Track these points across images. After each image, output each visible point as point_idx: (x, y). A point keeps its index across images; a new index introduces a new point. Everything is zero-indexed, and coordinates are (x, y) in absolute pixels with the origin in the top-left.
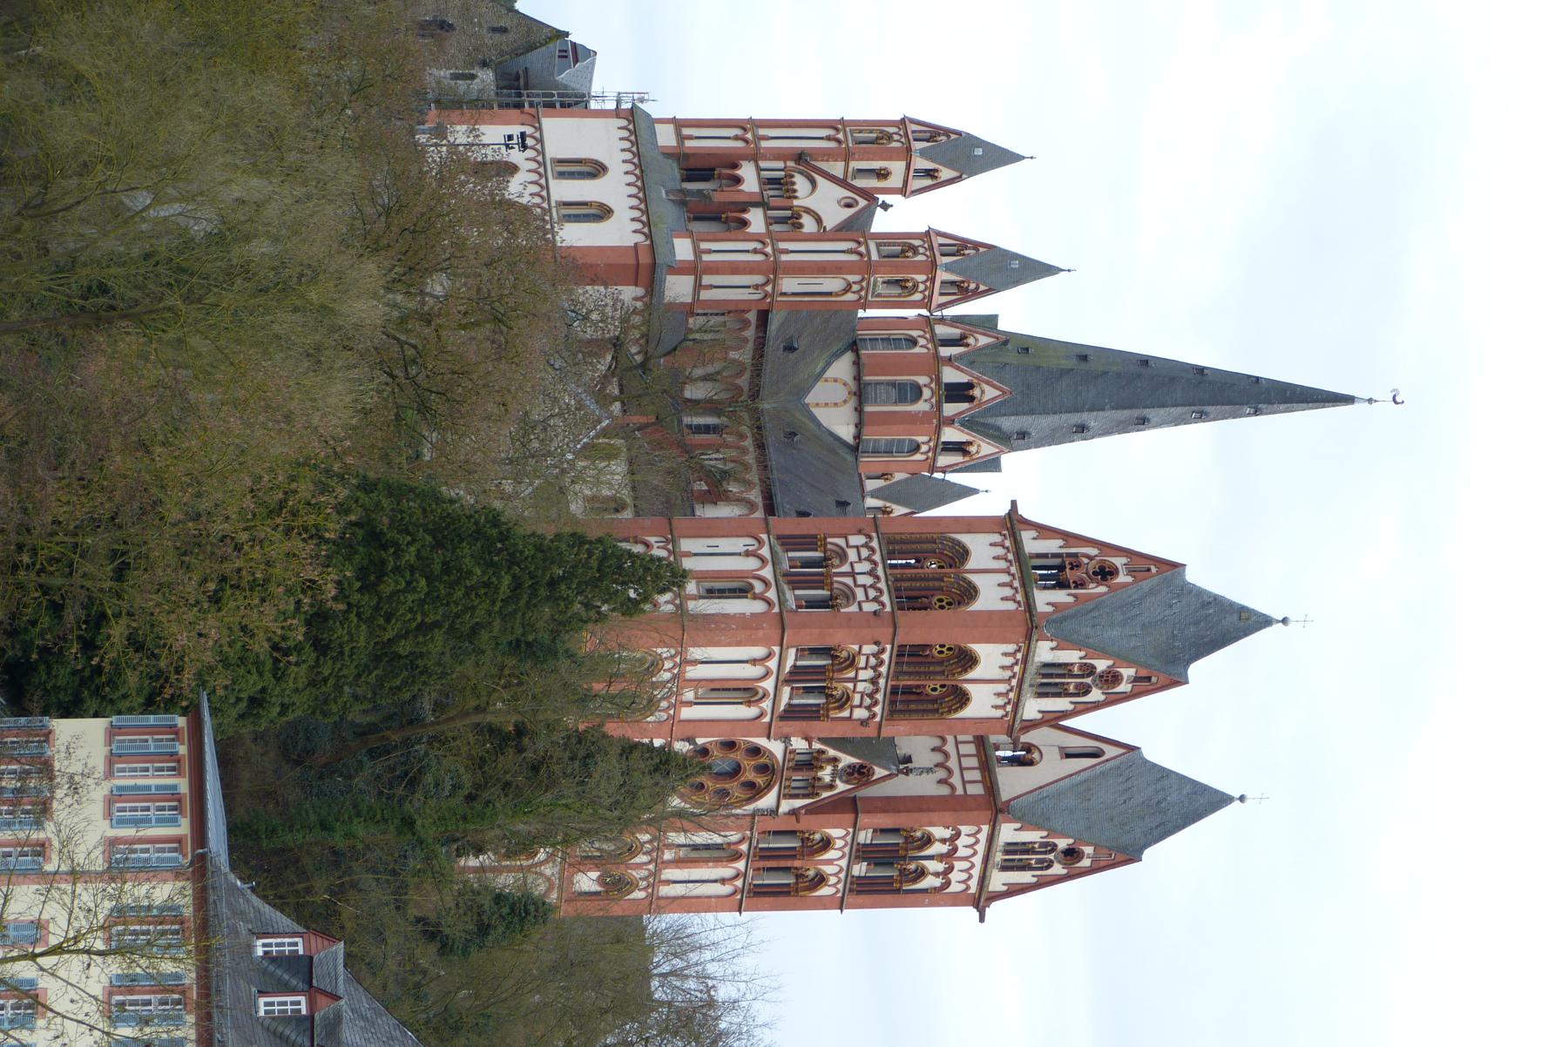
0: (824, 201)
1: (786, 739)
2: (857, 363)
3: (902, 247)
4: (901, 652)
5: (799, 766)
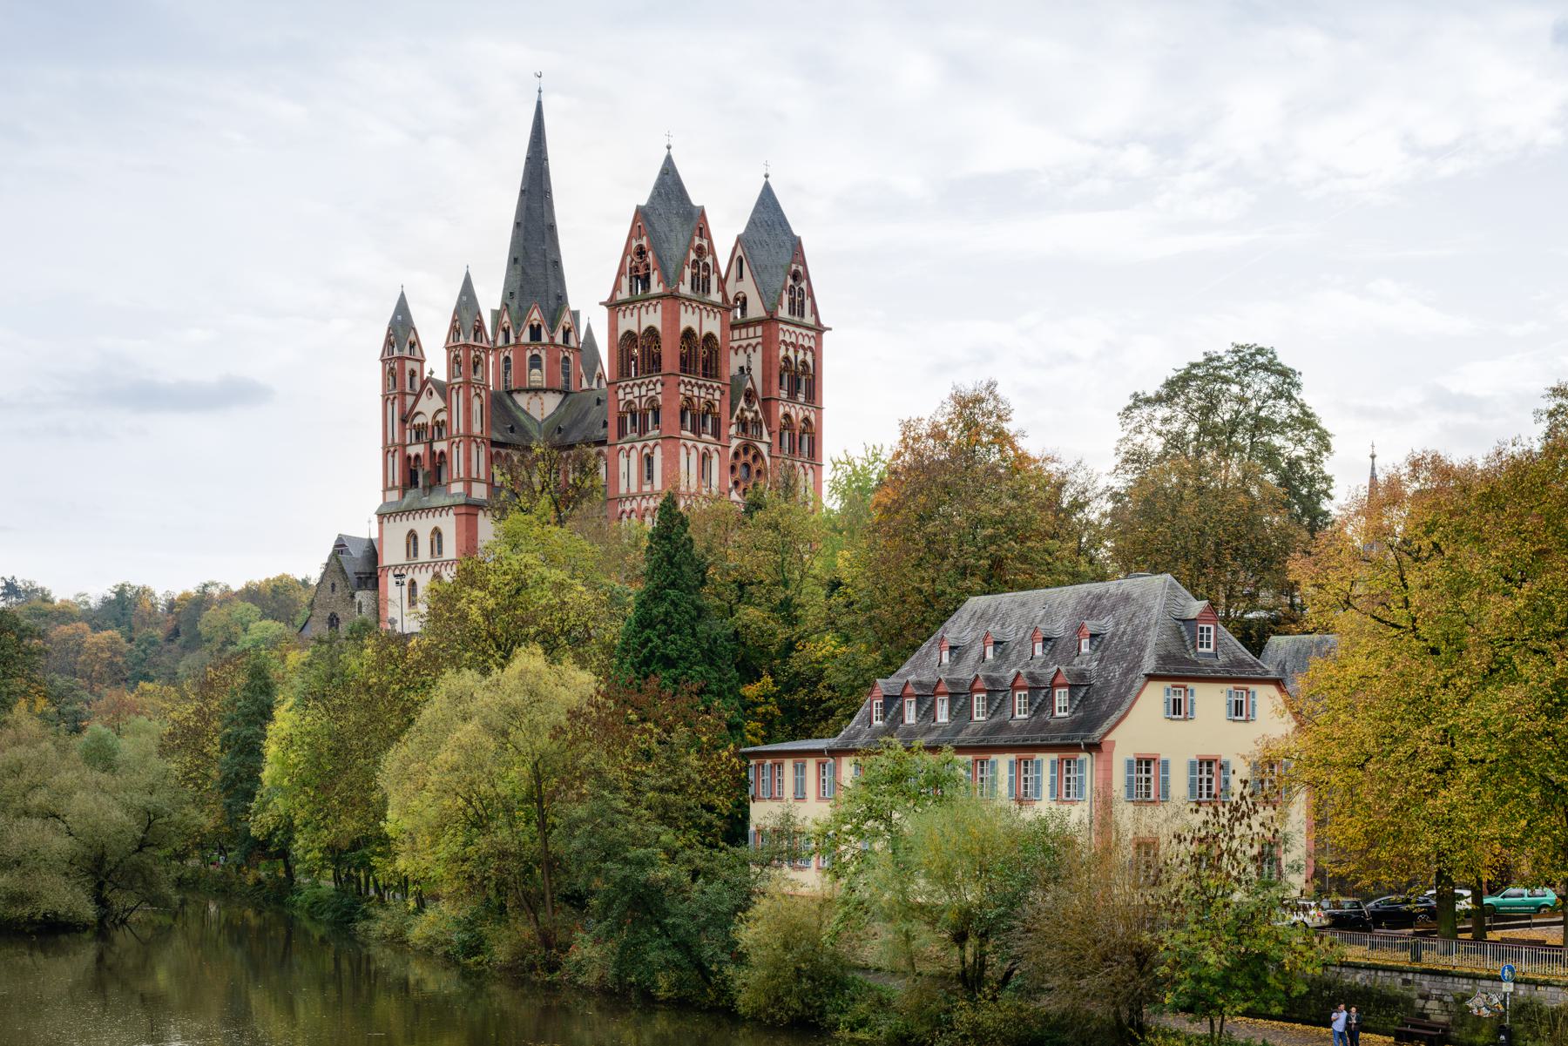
0: (429, 407)
1: (730, 437)
2: (519, 391)
3: (454, 362)
4: (684, 371)
5: (745, 430)
